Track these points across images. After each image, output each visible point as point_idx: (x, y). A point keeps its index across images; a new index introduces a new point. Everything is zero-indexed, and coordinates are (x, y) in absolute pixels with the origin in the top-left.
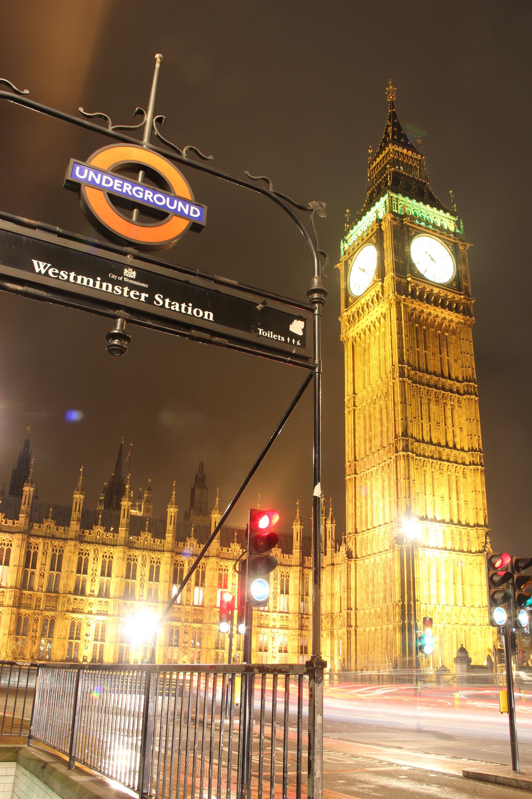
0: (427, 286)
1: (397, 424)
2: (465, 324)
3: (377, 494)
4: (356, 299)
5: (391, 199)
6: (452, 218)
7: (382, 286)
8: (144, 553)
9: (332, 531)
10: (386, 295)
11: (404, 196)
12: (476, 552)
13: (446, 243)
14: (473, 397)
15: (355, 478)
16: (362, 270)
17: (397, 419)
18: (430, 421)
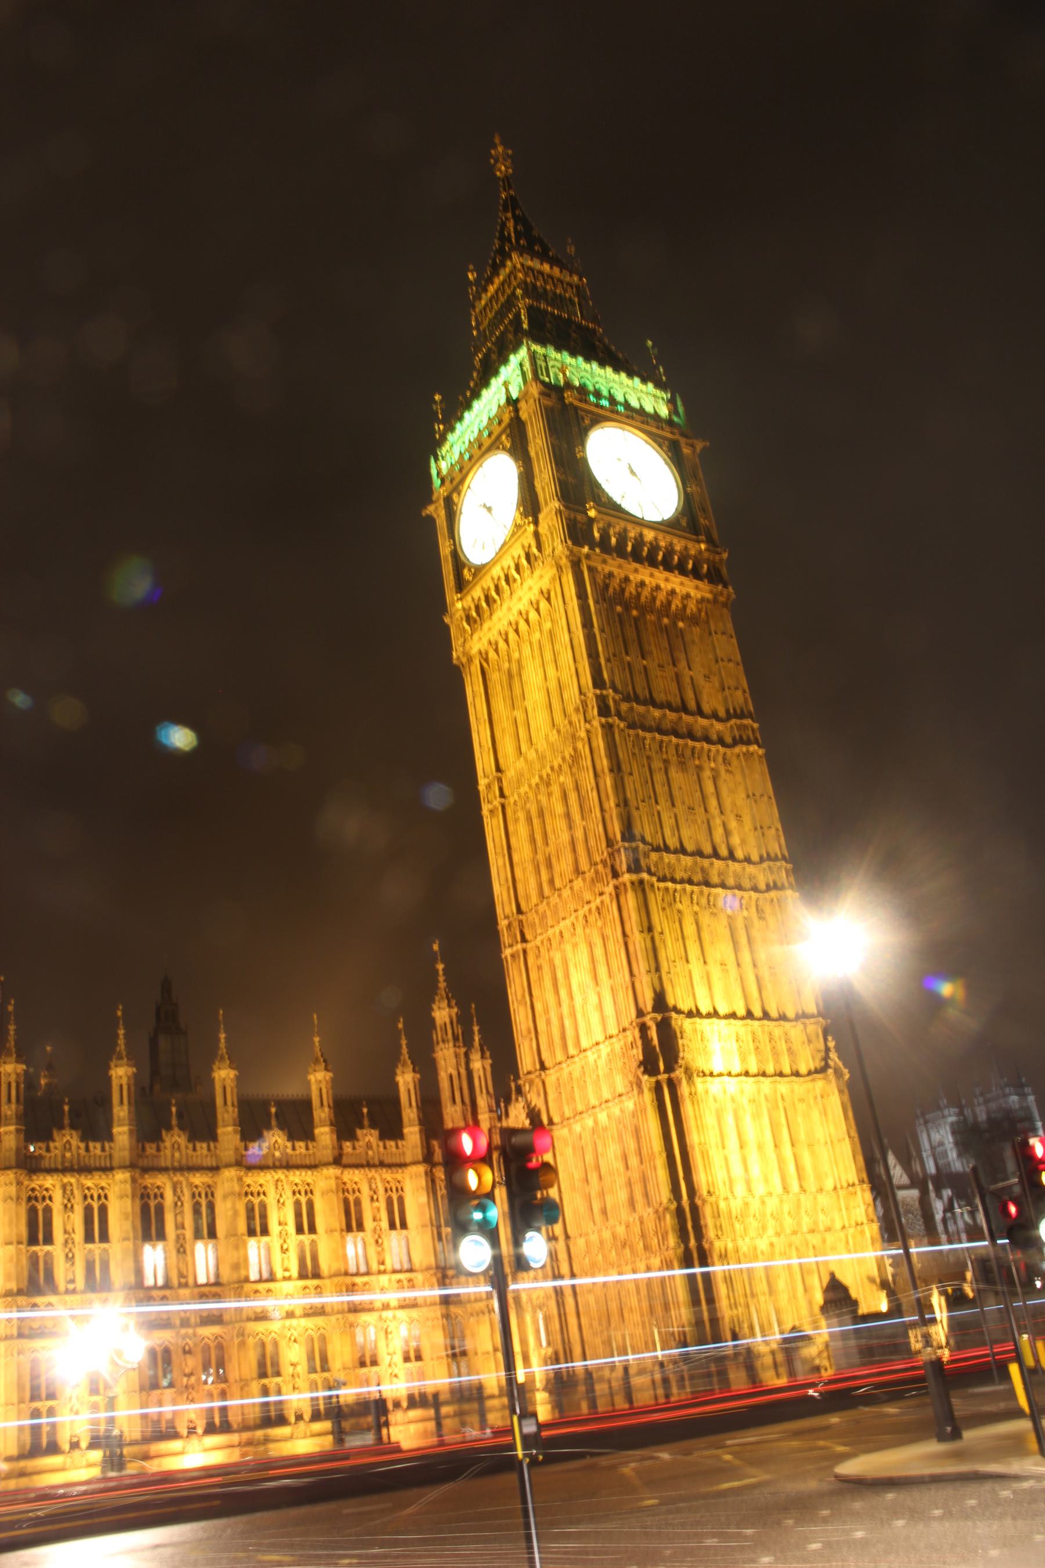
0: (629, 527)
1: (607, 816)
2: (715, 601)
3: (579, 977)
4: (479, 571)
5: (533, 357)
6: (658, 393)
7: (537, 535)
8: (65, 1180)
9: (485, 1075)
10: (548, 550)
11: (559, 349)
12: (810, 1073)
13: (655, 441)
14: (753, 748)
15: (525, 952)
16: (486, 508)
17: (606, 806)
18: (673, 805)
